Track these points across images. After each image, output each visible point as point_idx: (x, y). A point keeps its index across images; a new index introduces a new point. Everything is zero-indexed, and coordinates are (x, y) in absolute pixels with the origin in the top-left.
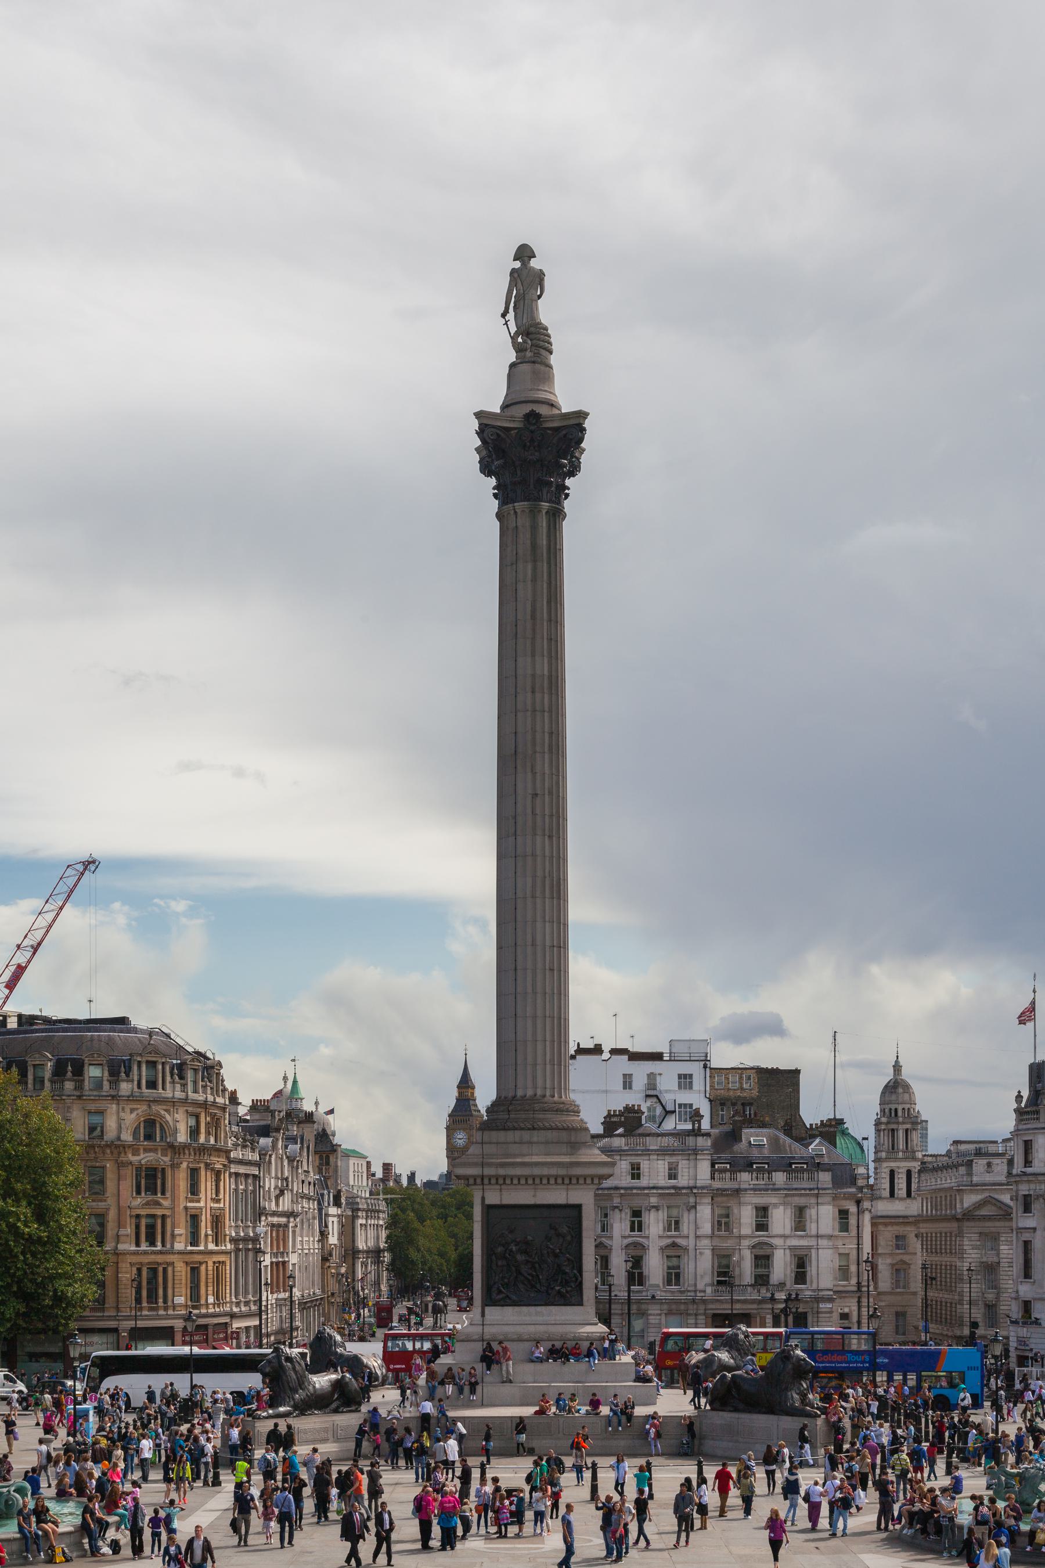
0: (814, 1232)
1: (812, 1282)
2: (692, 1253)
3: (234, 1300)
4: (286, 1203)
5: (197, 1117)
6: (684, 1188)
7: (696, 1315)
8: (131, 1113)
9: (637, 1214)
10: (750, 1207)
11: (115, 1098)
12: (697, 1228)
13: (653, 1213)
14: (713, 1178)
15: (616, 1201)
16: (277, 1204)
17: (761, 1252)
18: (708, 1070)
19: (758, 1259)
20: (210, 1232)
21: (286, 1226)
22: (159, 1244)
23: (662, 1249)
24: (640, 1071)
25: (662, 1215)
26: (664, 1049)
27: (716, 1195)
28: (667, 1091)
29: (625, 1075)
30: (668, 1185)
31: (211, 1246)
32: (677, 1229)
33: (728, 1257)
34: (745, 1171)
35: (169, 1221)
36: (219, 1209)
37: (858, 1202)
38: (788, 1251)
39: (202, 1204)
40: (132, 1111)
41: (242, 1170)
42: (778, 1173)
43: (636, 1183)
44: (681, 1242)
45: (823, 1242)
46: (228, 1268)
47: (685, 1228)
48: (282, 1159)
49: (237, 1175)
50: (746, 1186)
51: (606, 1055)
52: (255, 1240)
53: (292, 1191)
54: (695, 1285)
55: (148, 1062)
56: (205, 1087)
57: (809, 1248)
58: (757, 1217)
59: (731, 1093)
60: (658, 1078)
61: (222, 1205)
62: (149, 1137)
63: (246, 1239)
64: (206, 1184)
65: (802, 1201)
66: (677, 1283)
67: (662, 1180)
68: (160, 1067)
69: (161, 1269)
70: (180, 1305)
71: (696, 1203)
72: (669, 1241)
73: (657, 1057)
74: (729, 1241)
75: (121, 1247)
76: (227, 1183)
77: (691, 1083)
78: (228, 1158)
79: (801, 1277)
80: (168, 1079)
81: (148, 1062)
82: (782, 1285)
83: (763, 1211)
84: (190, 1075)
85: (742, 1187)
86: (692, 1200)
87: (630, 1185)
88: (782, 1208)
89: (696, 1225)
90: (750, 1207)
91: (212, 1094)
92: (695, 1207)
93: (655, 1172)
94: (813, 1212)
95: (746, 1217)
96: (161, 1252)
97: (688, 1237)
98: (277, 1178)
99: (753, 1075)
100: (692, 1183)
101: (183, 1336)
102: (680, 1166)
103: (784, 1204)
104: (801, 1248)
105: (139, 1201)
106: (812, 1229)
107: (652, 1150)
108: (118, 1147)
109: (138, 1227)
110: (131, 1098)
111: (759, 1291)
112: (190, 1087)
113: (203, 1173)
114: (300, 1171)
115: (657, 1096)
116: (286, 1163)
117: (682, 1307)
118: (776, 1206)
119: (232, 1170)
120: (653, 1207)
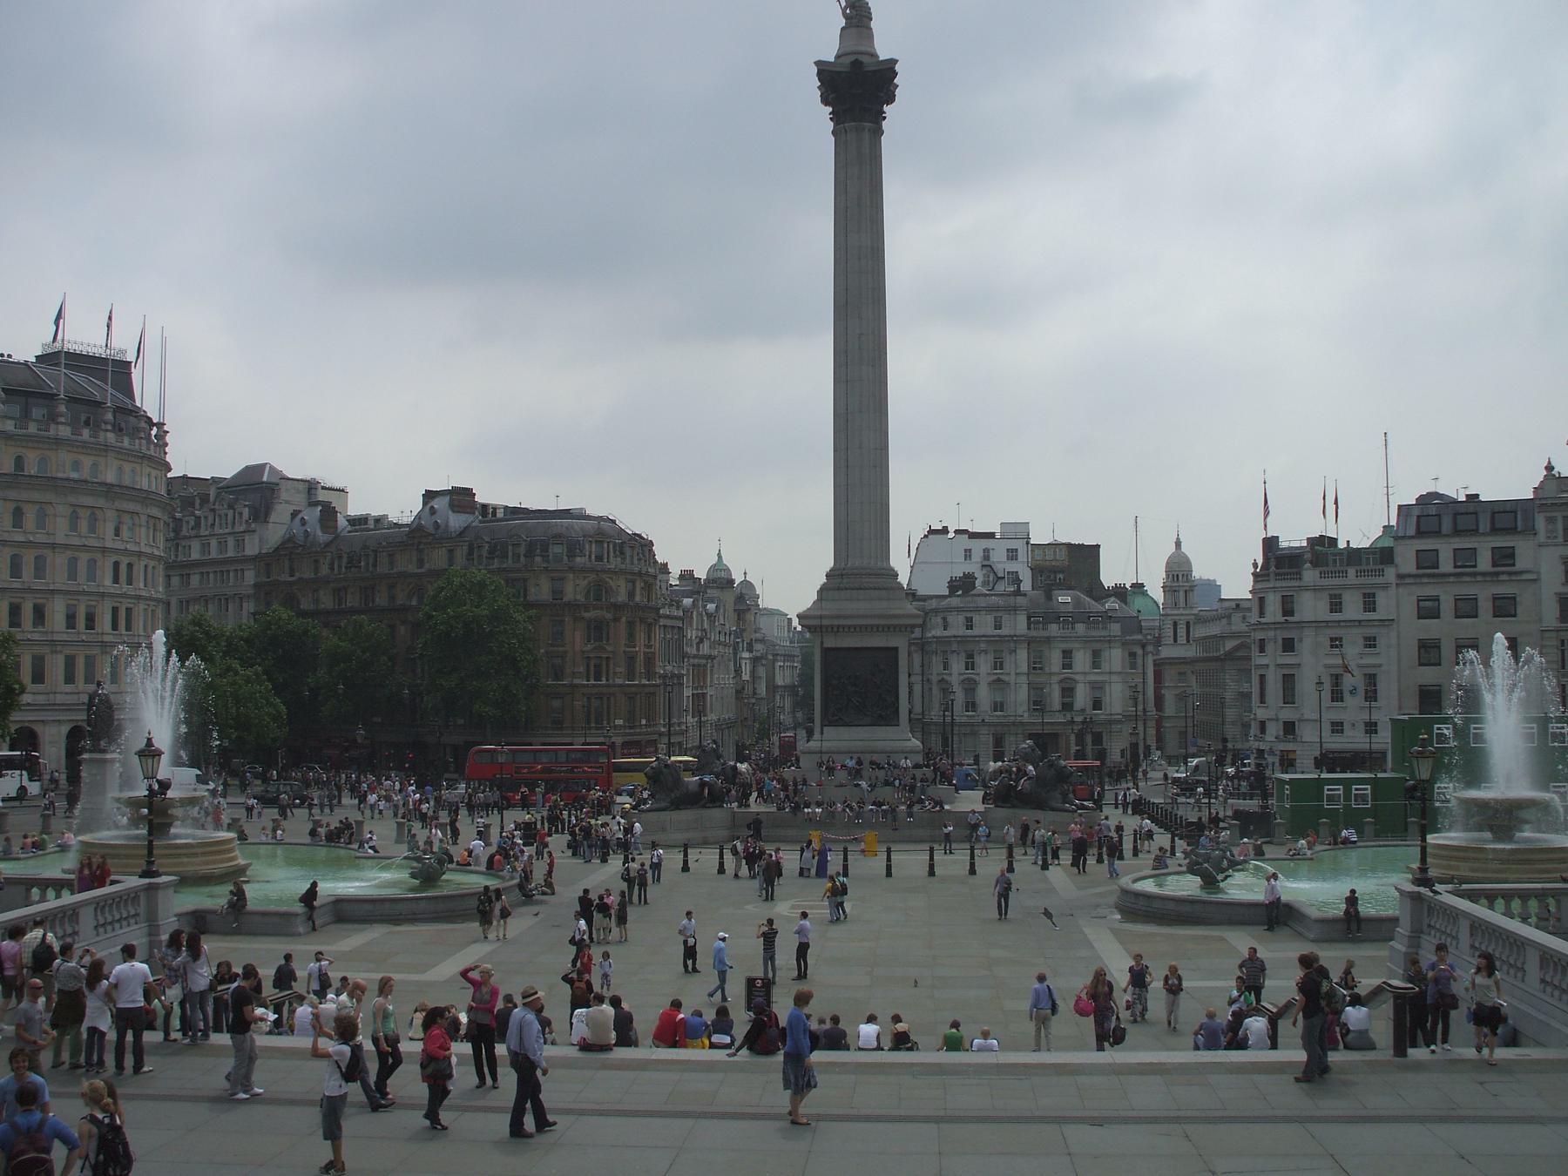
0: (1108, 670)
1: (1106, 709)
2: (1013, 687)
3: (662, 722)
4: (705, 649)
5: (633, 582)
6: (1006, 636)
7: (1017, 734)
8: (584, 580)
9: (970, 656)
11: (571, 569)
14: (1029, 628)
15: (954, 647)
16: (698, 650)
17: (1067, 686)
19: (1063, 690)
20: (643, 671)
21: (705, 666)
22: (604, 679)
24: (978, 546)
25: (991, 657)
26: (996, 529)
27: (1030, 642)
28: (999, 562)
29: (966, 550)
30: (994, 634)
31: (645, 682)
33: (1042, 689)
35: (612, 662)
36: (651, 652)
37: (1143, 646)
38: (1087, 685)
39: (637, 649)
40: (585, 578)
41: (669, 623)
43: (969, 632)
44: (1005, 678)
45: (1114, 678)
46: (657, 698)
47: (1006, 670)
48: (702, 615)
49: (665, 626)
50: (1056, 635)
51: (951, 535)
52: (680, 676)
53: (710, 639)
54: (1016, 711)
55: (596, 541)
56: (639, 560)
57: (1105, 682)
58: (1064, 658)
59: (1047, 563)
60: (991, 551)
61: (653, 650)
62: (598, 598)
63: (673, 676)
64: (641, 637)
65: (1097, 646)
67: (990, 631)
68: (606, 545)
69: (605, 699)
70: (621, 726)
72: (995, 677)
73: (991, 535)
75: (576, 681)
76: (658, 634)
77: (1017, 555)
78: (658, 613)
79: (1097, 704)
80: (612, 554)
81: (596, 541)
82: (1083, 710)
83: (1067, 654)
84: (628, 552)
86: (1012, 645)
87: (965, 634)
88: (1082, 652)
89: (1016, 663)
90: (1058, 651)
91: (645, 565)
92: (1015, 651)
93: (984, 625)
94: (1107, 654)
95: (1055, 659)
96: (608, 686)
98: (697, 629)
99: (1064, 549)
101: (622, 749)
103: (1084, 648)
104: (1095, 682)
105: (589, 647)
106: (1105, 667)
108: (573, 607)
109: (588, 666)
110: (584, 570)
111: (1064, 715)
112: (628, 561)
113: (638, 624)
114: (717, 624)
115: (991, 566)
116: (705, 618)
117: (1005, 728)
119: (661, 624)
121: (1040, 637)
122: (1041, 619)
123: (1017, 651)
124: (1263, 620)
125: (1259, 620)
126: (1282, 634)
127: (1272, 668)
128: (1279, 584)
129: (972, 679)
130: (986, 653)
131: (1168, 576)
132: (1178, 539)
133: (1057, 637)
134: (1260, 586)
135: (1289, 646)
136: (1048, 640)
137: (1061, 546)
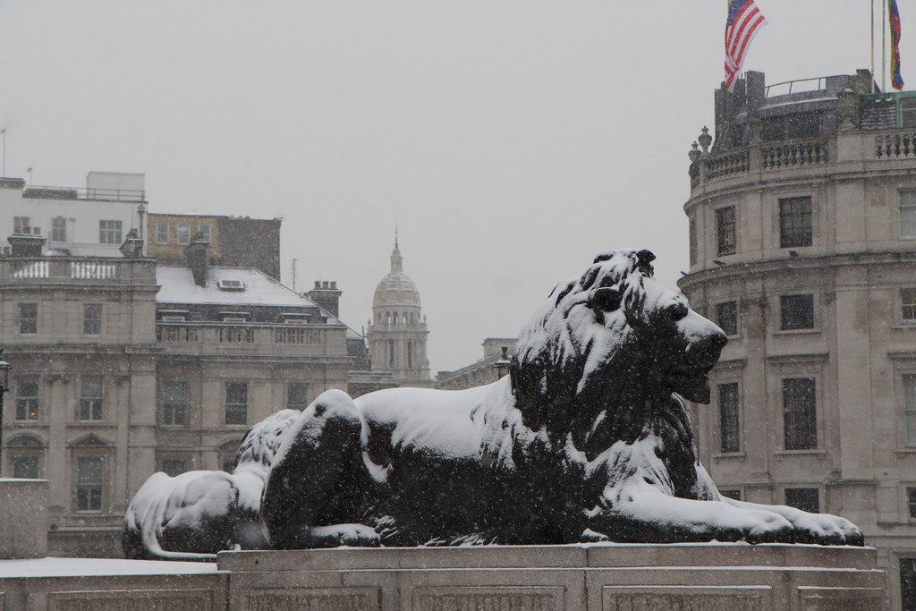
2: (121, 454)
12: (131, 412)
13: (58, 388)
18: (145, 216)
23: (72, 447)
26: (80, 185)
28: (83, 245)
32: (97, 416)
44: (101, 435)
47: (112, 413)
60: (69, 227)
66: (96, 505)
72: (83, 434)
73: (70, 195)
83: (237, 391)
85: (209, 350)
86: (124, 369)
87: (20, 341)
88: (268, 385)
89: (130, 405)
90: (218, 385)
92: (127, 378)
99: (212, 225)
102: (104, 311)
103: (273, 380)
118: (258, 382)
120: (57, 377)
123: (134, 379)
124: (728, 260)
125: (718, 259)
126: (774, 290)
127: (754, 368)
128: (770, 174)
129: (33, 439)
130: (66, 382)
131: (378, 316)
132: (396, 252)
134: (716, 185)
135: (799, 313)
136: (196, 363)
137: (205, 221)
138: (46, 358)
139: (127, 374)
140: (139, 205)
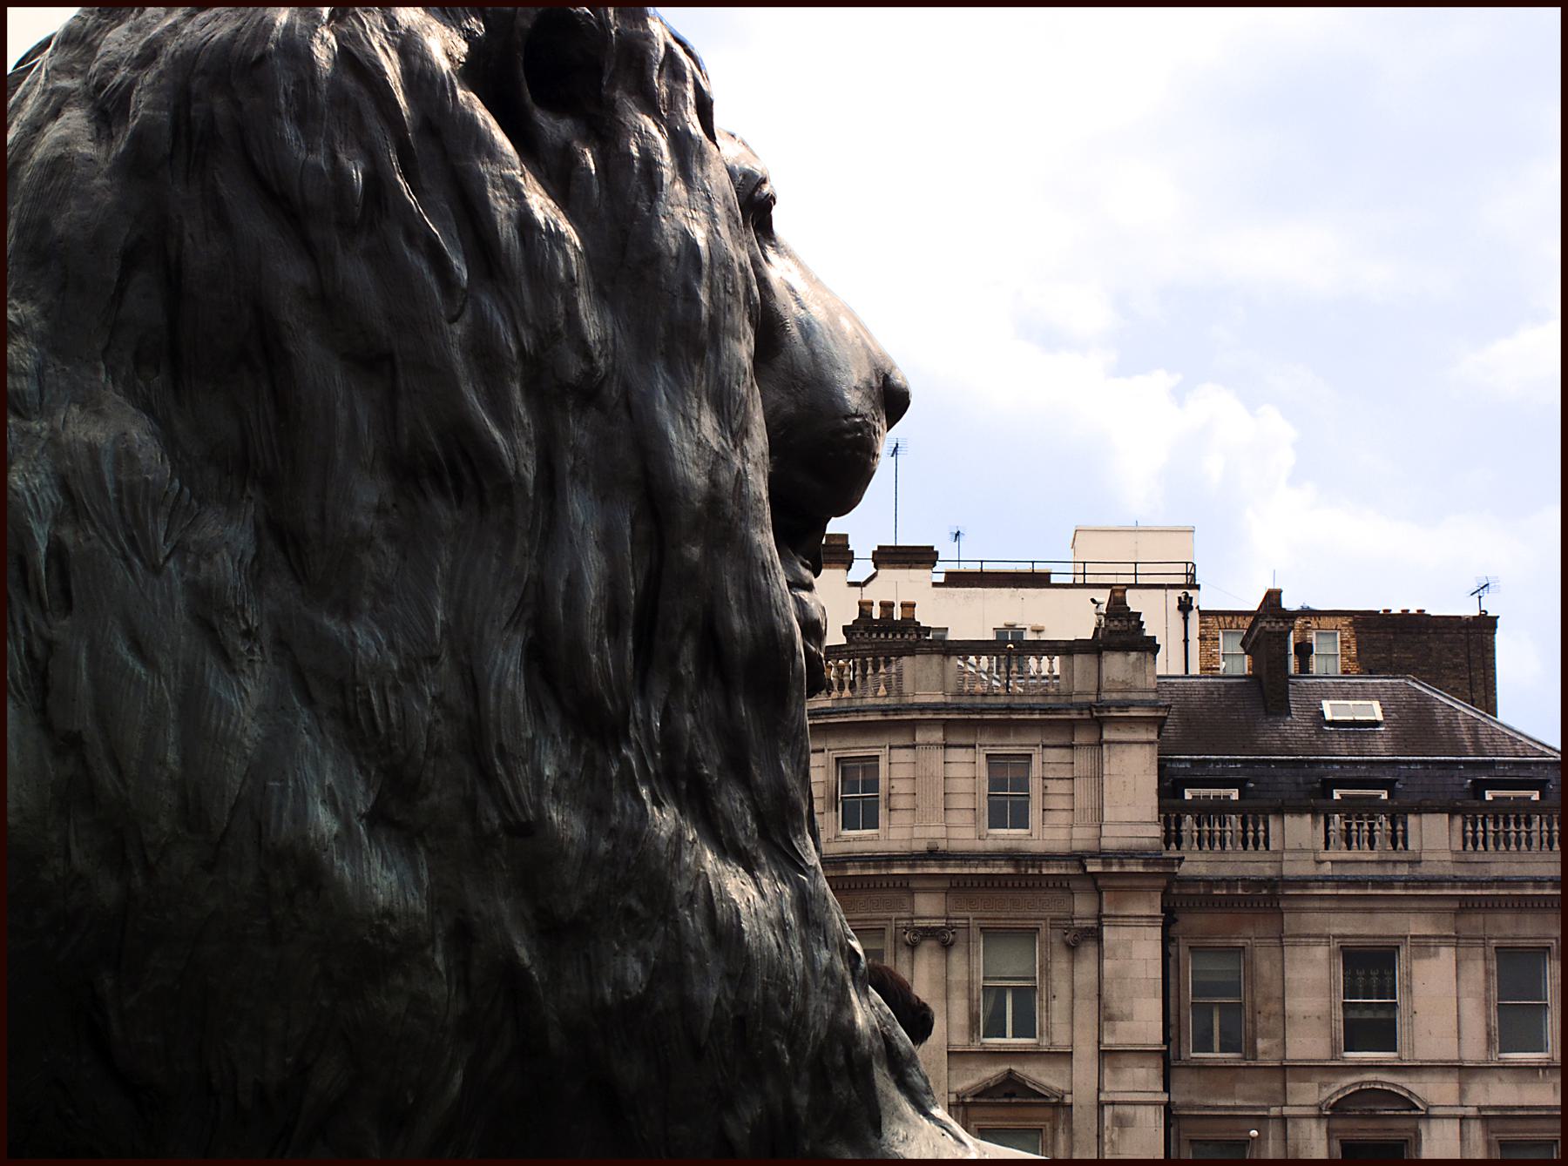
10: (1321, 952)
12: (1105, 1016)
18: (1194, 617)
30: (990, 845)
32: (1025, 1027)
34: (1299, 811)
42: (1427, 819)
50: (1304, 869)
71: (1099, 917)
72: (991, 1072)
73: (1038, 580)
74: (1239, 1087)
85: (1292, 869)
86: (1083, 907)
88: (1447, 955)
90: (1321, 952)
92: (1095, 935)
97: (1068, 1056)
100: (1082, 838)
103: (1457, 940)
107: (923, 708)
118: (1424, 946)
120: (929, 933)
121: (1229, 882)
122: (1235, 795)
123: (1107, 933)
130: (947, 947)
133: (1324, 881)
138: (906, 886)
139: (1091, 923)
140: (1180, 593)
